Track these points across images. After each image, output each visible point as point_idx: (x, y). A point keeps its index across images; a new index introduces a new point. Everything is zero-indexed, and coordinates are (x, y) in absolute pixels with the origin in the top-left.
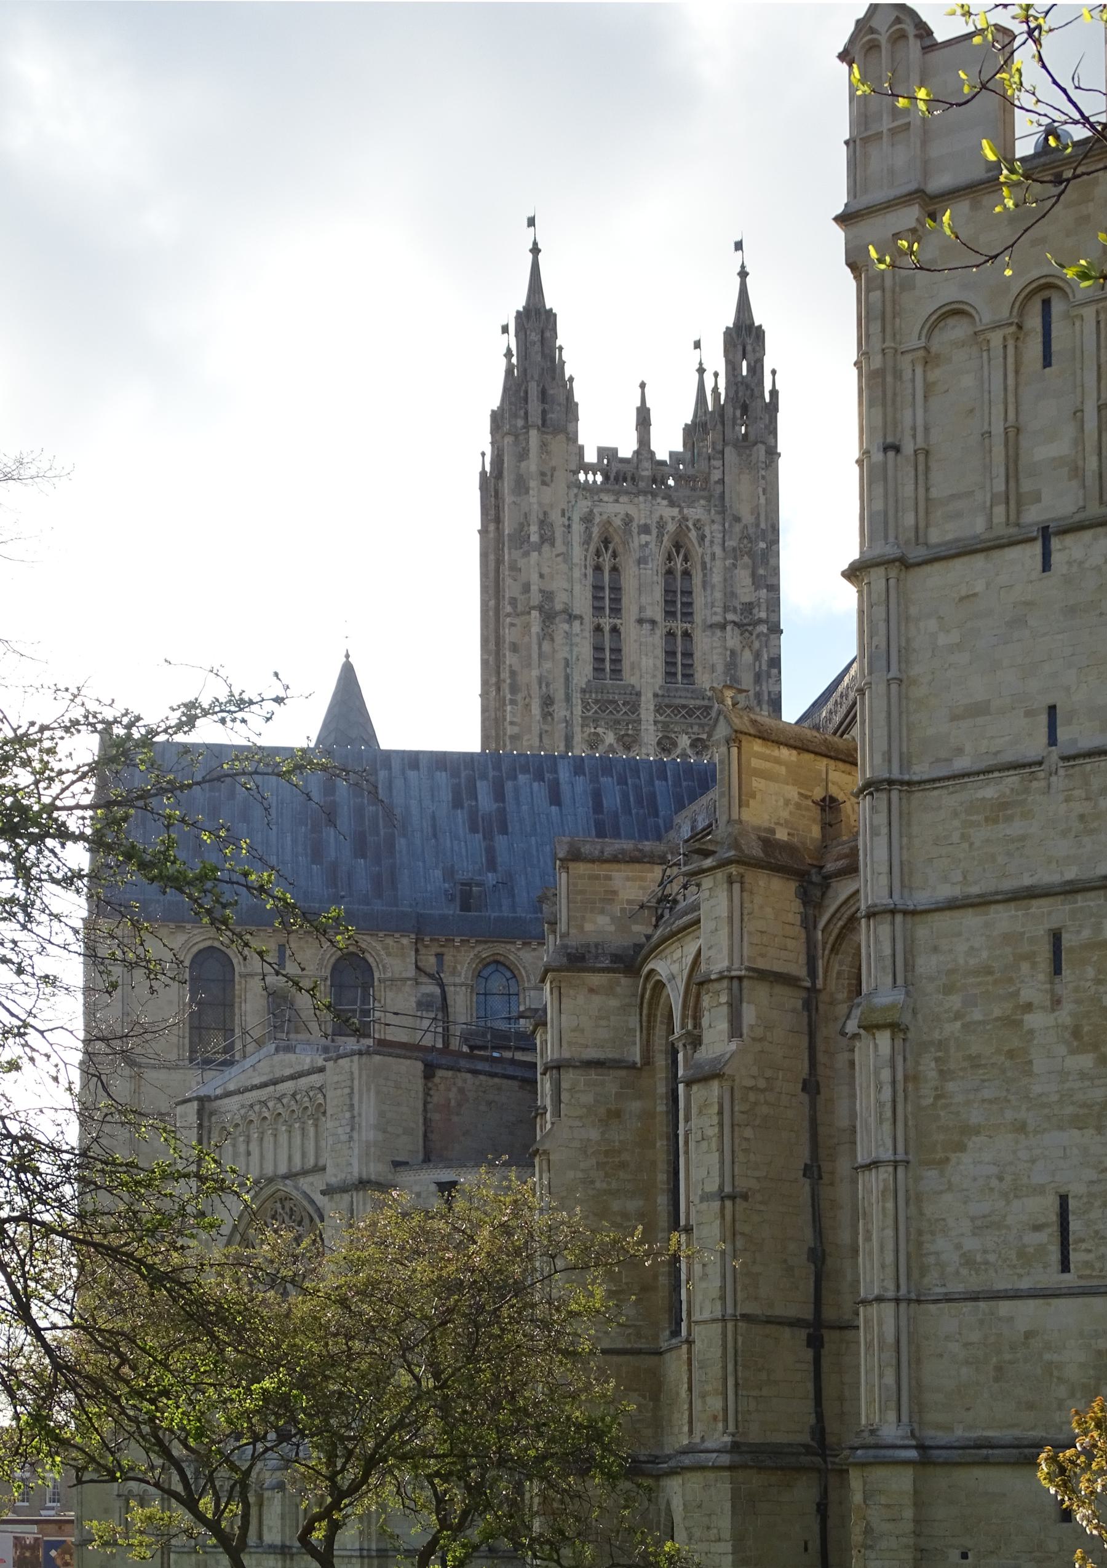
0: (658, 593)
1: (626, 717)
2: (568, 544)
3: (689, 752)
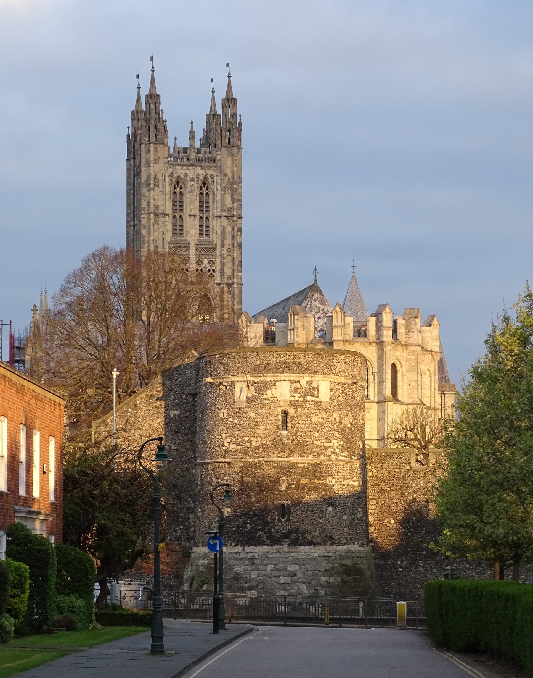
0: (197, 204)
1: (184, 253)
2: (164, 186)
3: (208, 265)
